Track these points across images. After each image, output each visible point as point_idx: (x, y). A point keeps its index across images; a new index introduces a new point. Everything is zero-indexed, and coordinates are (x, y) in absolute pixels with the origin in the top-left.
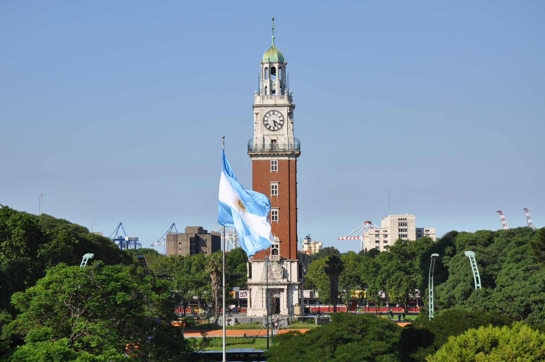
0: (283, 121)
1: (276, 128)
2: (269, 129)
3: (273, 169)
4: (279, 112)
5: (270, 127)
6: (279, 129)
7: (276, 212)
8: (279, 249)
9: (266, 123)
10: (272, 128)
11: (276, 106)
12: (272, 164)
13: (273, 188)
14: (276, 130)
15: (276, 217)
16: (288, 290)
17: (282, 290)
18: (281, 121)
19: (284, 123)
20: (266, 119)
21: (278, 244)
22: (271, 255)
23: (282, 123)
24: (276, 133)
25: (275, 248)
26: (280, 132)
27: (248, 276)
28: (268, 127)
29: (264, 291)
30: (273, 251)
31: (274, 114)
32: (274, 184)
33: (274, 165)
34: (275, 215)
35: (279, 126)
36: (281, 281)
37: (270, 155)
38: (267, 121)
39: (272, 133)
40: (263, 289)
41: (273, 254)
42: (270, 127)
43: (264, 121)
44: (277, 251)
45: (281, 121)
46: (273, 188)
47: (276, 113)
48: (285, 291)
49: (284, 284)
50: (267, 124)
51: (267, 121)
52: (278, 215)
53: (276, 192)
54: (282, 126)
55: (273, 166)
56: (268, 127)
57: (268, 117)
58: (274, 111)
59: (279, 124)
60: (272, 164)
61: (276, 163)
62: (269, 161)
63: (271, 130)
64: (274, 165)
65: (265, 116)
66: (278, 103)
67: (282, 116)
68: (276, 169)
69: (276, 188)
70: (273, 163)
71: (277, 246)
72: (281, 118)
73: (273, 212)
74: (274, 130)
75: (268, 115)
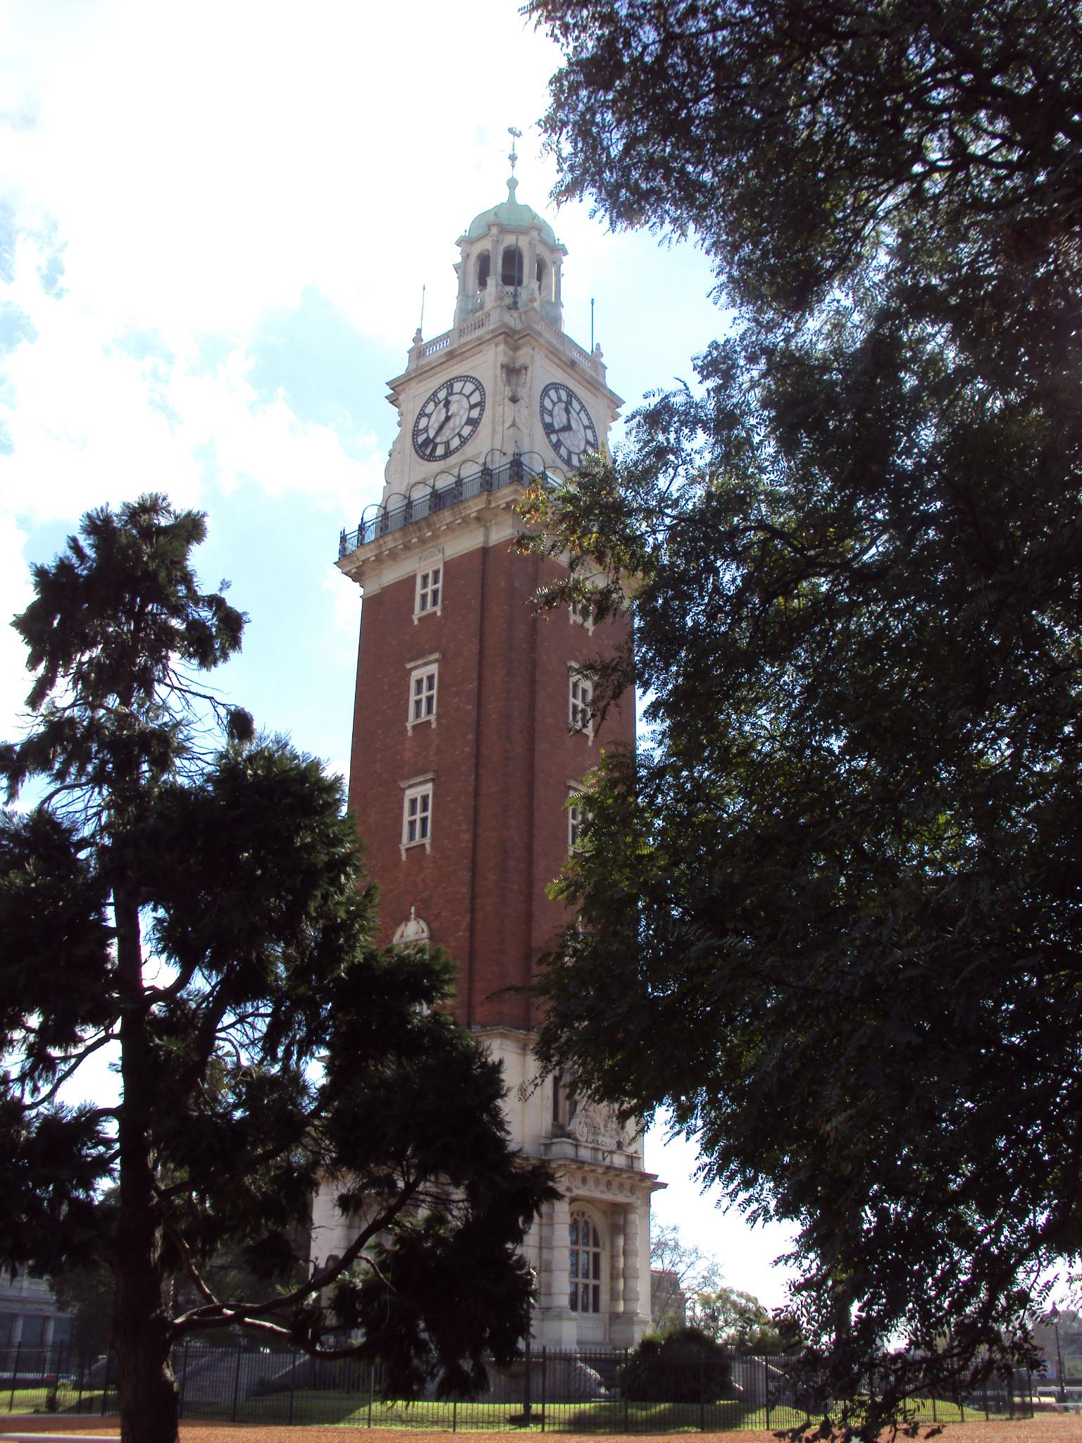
0: (481, 404)
4: (466, 379)
6: (464, 441)
7: (425, 798)
9: (420, 440)
20: (423, 423)
23: (475, 413)
24: (453, 460)
35: (467, 431)
45: (472, 407)
47: (457, 387)
57: (429, 416)
58: (449, 385)
60: (425, 585)
67: (479, 387)
70: (425, 578)
72: (476, 398)
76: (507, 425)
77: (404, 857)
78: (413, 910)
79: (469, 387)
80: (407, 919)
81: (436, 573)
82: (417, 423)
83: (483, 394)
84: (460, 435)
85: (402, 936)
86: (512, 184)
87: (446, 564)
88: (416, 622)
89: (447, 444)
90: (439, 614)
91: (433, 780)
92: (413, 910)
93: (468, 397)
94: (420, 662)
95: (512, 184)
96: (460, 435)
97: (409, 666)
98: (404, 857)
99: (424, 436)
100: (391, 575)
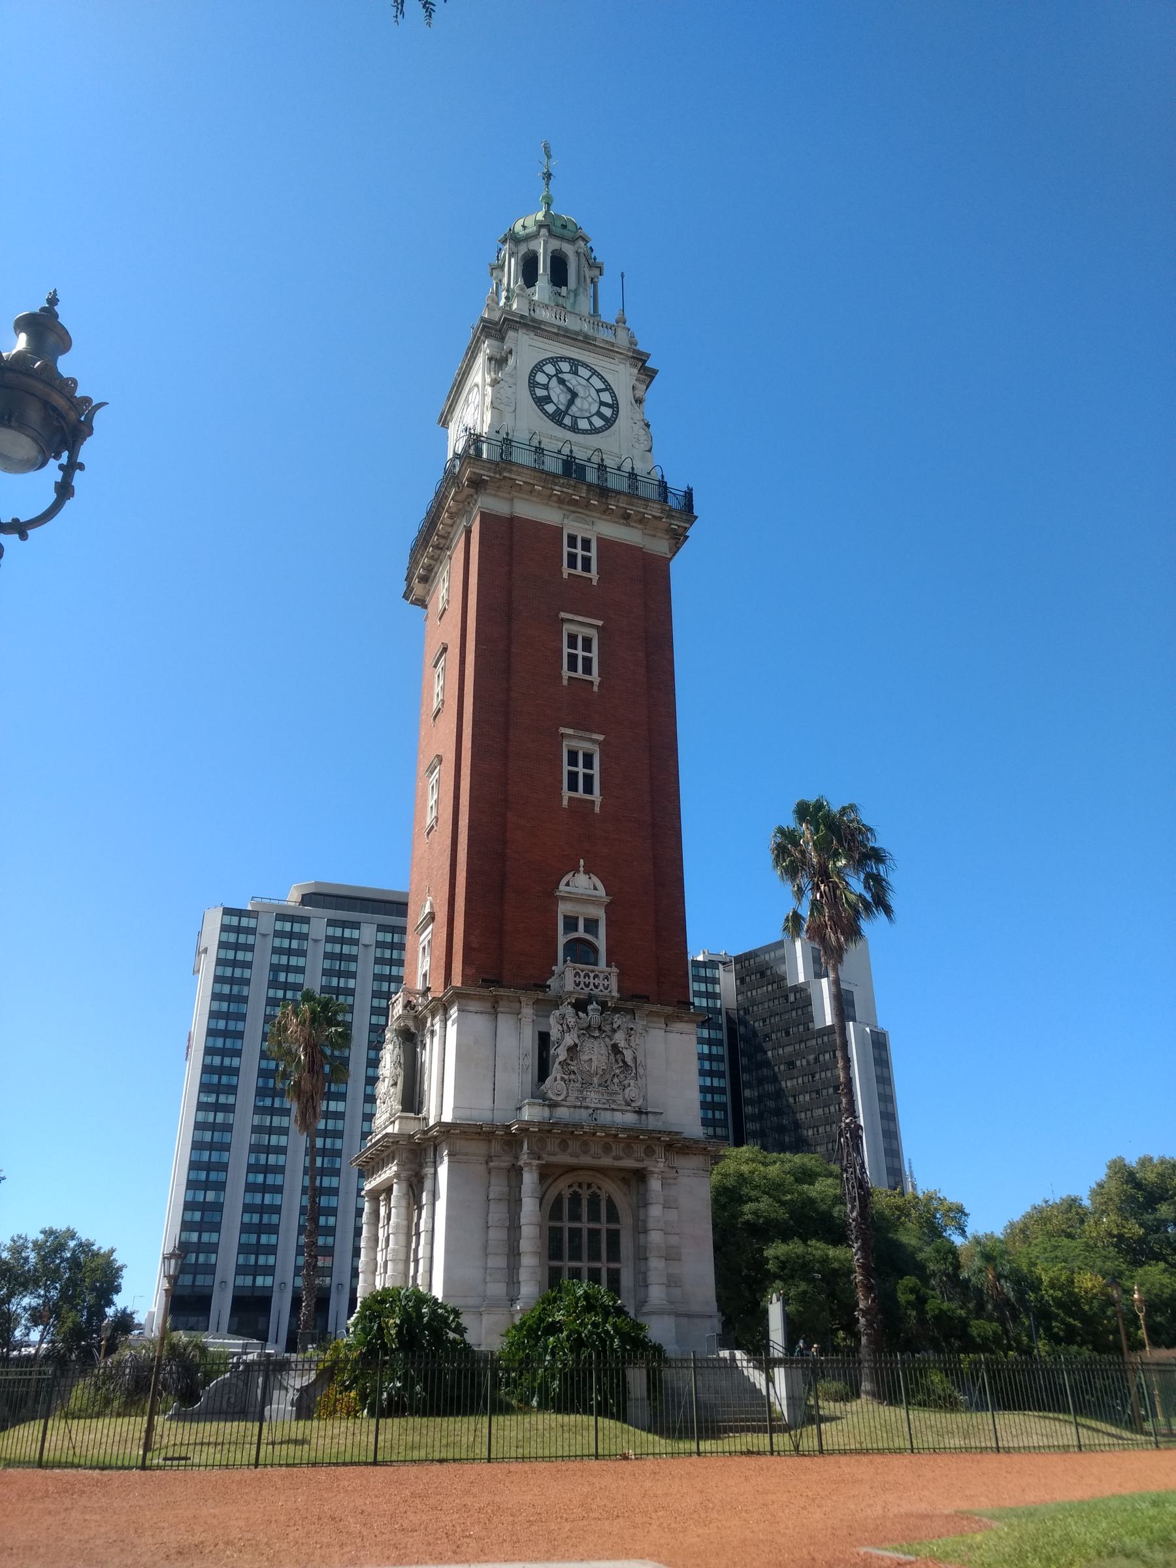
0: (615, 406)
1: (583, 424)
4: (594, 372)
6: (595, 431)
8: (601, 943)
9: (540, 393)
14: (585, 432)
15: (588, 779)
18: (602, 403)
19: (616, 413)
21: (600, 914)
23: (607, 412)
24: (580, 438)
25: (581, 933)
28: (550, 408)
30: (569, 945)
31: (576, 373)
32: (582, 632)
34: (581, 770)
35: (598, 422)
38: (546, 387)
43: (533, 384)
44: (595, 950)
47: (582, 371)
48: (655, 1184)
50: (548, 400)
51: (546, 387)
53: (587, 669)
54: (609, 422)
58: (575, 364)
65: (538, 367)
67: (608, 388)
69: (587, 646)
70: (572, 541)
71: (591, 925)
72: (606, 397)
77: (565, 803)
78: (582, 862)
79: (600, 385)
82: (532, 375)
83: (614, 396)
84: (591, 423)
85: (568, 884)
87: (600, 540)
88: (565, 576)
89: (575, 419)
90: (595, 583)
91: (600, 743)
92: (582, 862)
93: (598, 391)
94: (580, 619)
96: (591, 423)
97: (563, 615)
98: (565, 803)
99: (545, 393)
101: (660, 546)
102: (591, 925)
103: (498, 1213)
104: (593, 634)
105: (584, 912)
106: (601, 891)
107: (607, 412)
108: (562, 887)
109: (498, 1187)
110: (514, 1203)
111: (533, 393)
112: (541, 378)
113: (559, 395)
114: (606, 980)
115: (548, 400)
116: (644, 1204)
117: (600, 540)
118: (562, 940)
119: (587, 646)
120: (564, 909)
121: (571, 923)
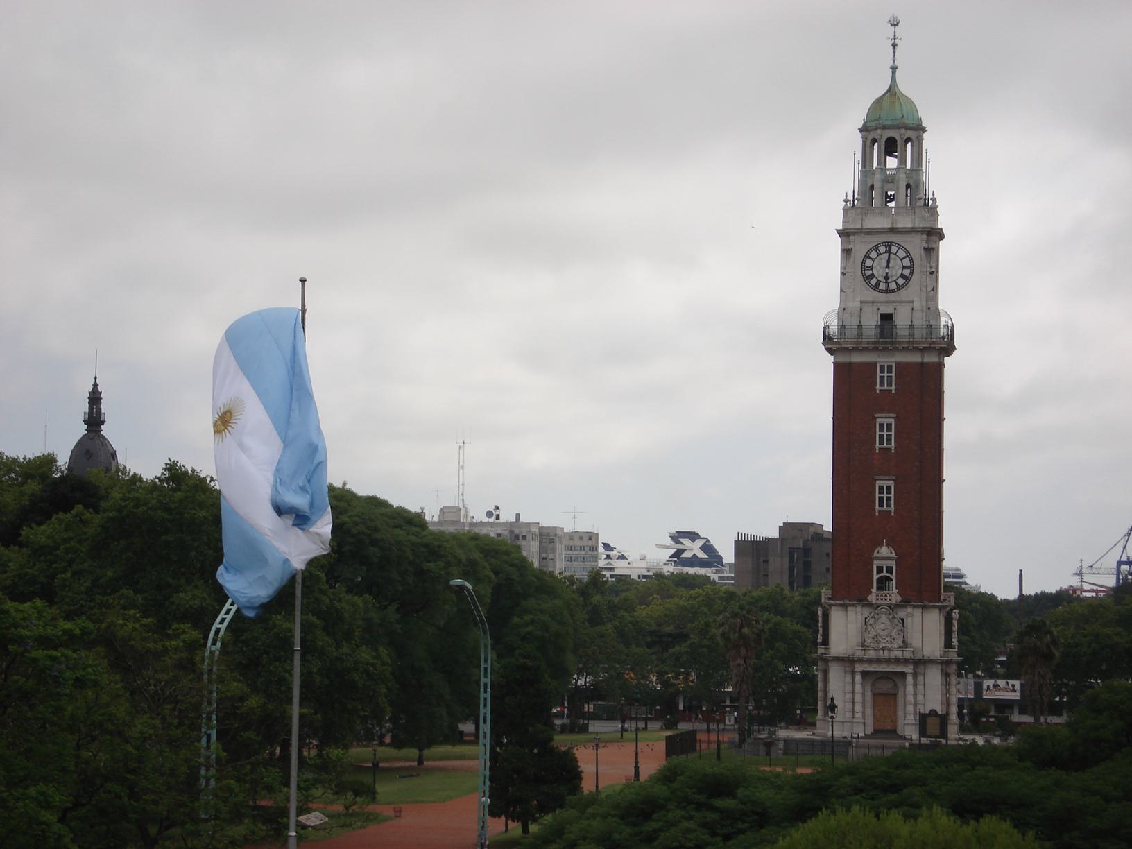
0: (911, 267)
2: (876, 288)
3: (882, 384)
4: (900, 247)
5: (878, 282)
6: (899, 288)
7: (889, 488)
8: (894, 577)
9: (868, 273)
10: (882, 286)
11: (892, 230)
12: (882, 371)
13: (881, 429)
14: (893, 291)
15: (889, 499)
16: (915, 675)
17: (903, 675)
18: (904, 267)
19: (912, 273)
21: (893, 564)
22: (874, 590)
23: (907, 272)
24: (892, 297)
25: (885, 573)
26: (903, 295)
27: (820, 639)
28: (873, 282)
29: (858, 678)
30: (879, 580)
33: (886, 374)
34: (885, 495)
35: (901, 281)
36: (897, 653)
37: (875, 349)
39: (882, 297)
40: (853, 673)
41: (879, 588)
42: (878, 282)
43: (864, 268)
45: (904, 267)
46: (881, 429)
48: (910, 679)
49: (906, 662)
50: (872, 276)
52: (892, 495)
53: (889, 440)
54: (907, 279)
55: (882, 378)
56: (873, 282)
57: (873, 260)
58: (889, 245)
59: (902, 276)
60: (882, 371)
61: (890, 371)
62: (875, 364)
63: (879, 291)
64: (886, 374)
65: (867, 256)
66: (899, 225)
67: (909, 255)
68: (890, 384)
69: (889, 429)
71: (889, 570)
72: (907, 262)
73: (881, 488)
74: (887, 291)
75: (873, 255)
76: (929, 289)
79: (902, 254)
80: (881, 545)
81: (890, 368)
83: (912, 261)
86: (894, 69)
95: (894, 69)
100: (857, 358)
101: (931, 358)
102: (889, 570)
103: (849, 688)
104: (892, 421)
105: (885, 564)
106: (894, 555)
107: (907, 272)
108: (875, 554)
109: (849, 678)
110: (853, 683)
111: (863, 274)
112: (869, 263)
113: (879, 272)
114: (894, 595)
115: (872, 276)
116: (905, 686)
117: (897, 364)
118: (876, 577)
119: (889, 429)
120: (876, 563)
121: (880, 570)
